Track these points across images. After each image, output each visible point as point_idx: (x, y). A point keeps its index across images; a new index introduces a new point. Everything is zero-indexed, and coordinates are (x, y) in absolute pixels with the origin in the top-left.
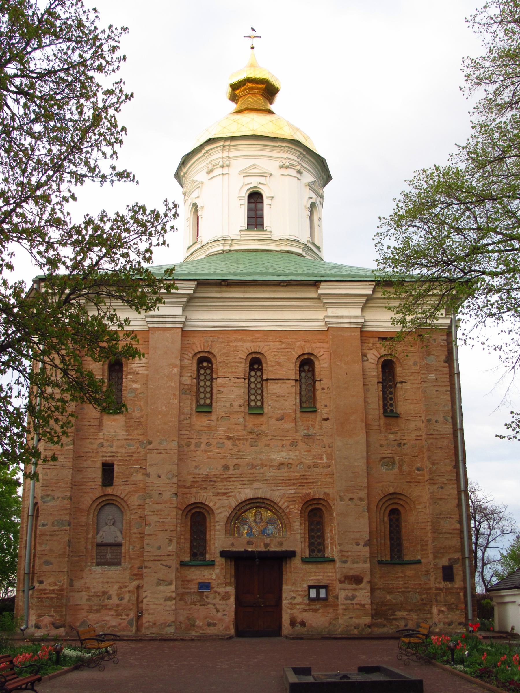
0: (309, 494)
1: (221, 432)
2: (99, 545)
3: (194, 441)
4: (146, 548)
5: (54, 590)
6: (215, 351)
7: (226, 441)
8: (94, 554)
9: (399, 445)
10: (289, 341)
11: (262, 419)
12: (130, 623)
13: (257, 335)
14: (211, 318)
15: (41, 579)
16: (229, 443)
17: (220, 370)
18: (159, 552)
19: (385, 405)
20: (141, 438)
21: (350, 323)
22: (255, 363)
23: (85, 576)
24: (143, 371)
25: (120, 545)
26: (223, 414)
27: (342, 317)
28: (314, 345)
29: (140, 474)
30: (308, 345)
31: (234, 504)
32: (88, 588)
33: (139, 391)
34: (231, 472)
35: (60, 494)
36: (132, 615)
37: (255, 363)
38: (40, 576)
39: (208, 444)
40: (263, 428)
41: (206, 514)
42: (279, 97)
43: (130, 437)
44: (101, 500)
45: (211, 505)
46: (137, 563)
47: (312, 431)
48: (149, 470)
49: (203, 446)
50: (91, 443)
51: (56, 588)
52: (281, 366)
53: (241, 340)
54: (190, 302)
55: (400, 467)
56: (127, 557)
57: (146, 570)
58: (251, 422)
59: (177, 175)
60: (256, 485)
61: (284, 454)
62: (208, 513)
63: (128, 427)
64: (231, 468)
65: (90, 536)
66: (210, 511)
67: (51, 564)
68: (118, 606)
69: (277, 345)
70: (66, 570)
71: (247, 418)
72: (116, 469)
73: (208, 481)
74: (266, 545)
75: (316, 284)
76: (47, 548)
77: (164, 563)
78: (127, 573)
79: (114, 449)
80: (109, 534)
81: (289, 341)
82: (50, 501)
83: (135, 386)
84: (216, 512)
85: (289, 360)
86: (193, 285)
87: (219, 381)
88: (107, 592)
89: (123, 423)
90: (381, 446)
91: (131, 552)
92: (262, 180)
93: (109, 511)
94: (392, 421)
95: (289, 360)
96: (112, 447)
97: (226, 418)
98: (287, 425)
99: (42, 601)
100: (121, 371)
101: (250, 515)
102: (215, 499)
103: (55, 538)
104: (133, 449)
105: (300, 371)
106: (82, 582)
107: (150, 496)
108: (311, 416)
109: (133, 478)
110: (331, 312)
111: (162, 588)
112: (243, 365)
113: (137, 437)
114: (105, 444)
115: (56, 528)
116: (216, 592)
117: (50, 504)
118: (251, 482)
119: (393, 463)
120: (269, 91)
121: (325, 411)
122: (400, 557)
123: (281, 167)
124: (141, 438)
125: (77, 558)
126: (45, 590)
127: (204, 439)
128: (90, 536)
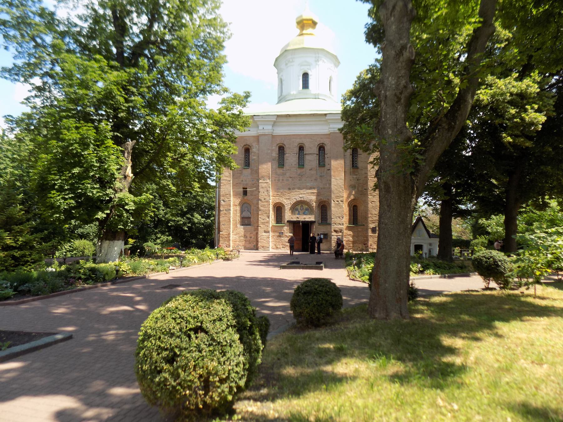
1: (288, 174)
6: (285, 143)
9: (358, 180)
11: (304, 170)
12: (254, 246)
14: (282, 130)
16: (290, 179)
17: (287, 150)
19: (353, 164)
22: (301, 148)
24: (257, 152)
25: (250, 218)
36: (255, 243)
37: (301, 148)
39: (283, 180)
42: (317, 26)
46: (256, 225)
52: (311, 149)
54: (274, 124)
55: (358, 189)
58: (299, 171)
59: (274, 65)
61: (312, 184)
66: (284, 206)
74: (305, 218)
75: (326, 115)
78: (253, 228)
80: (246, 214)
83: (254, 157)
86: (276, 117)
87: (287, 155)
92: (308, 67)
93: (245, 205)
98: (313, 172)
100: (249, 152)
101: (299, 207)
102: (285, 201)
104: (254, 182)
105: (319, 150)
107: (261, 200)
108: (323, 168)
110: (331, 126)
112: (295, 149)
119: (355, 187)
120: (314, 24)
121: (328, 166)
122: (357, 224)
123: (316, 61)
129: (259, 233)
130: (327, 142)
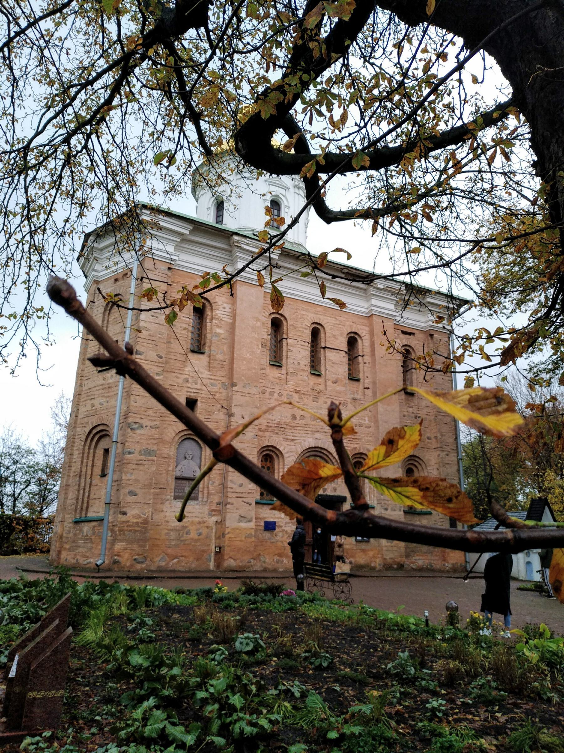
0: (355, 448)
1: (291, 384)
2: (177, 478)
3: (268, 390)
4: (230, 484)
5: (137, 523)
7: (294, 394)
8: (173, 487)
10: (341, 319)
11: (320, 380)
13: (319, 309)
15: (124, 510)
18: (240, 490)
20: (224, 380)
21: (388, 314)
22: (315, 333)
23: (165, 510)
26: (292, 370)
27: (383, 308)
28: (359, 327)
29: (221, 413)
30: (355, 325)
31: (300, 451)
32: (168, 522)
33: (222, 336)
34: (297, 421)
35: (149, 423)
38: (124, 507)
40: (321, 387)
41: (274, 456)
43: (213, 377)
44: (183, 434)
45: (281, 449)
47: (356, 396)
48: (234, 410)
49: (276, 395)
50: (177, 377)
51: (140, 520)
53: (307, 310)
56: (206, 492)
57: (228, 506)
58: (313, 380)
60: (317, 435)
62: (277, 455)
63: (210, 367)
64: (298, 418)
65: (170, 469)
67: (136, 495)
68: (196, 541)
69: (333, 321)
70: (151, 502)
71: (310, 376)
72: (199, 404)
73: (279, 427)
76: (133, 477)
77: (245, 500)
78: (206, 509)
79: (198, 386)
81: (341, 319)
82: (138, 428)
83: (218, 331)
84: (286, 455)
85: (342, 335)
87: (289, 340)
88: (186, 527)
89: (206, 363)
90: (404, 416)
91: (211, 488)
92: (283, 191)
94: (410, 398)
95: (342, 335)
96: (196, 384)
97: (295, 374)
99: (124, 534)
103: (141, 468)
106: (162, 515)
109: (214, 417)
110: (374, 302)
111: (243, 525)
113: (220, 378)
114: (190, 380)
115: (143, 457)
116: (283, 531)
117: (138, 432)
118: (313, 432)
124: (224, 380)
125: (158, 490)
126: (128, 522)
127: (277, 390)
128: (170, 469)
129: (228, 523)
130: (363, 331)
